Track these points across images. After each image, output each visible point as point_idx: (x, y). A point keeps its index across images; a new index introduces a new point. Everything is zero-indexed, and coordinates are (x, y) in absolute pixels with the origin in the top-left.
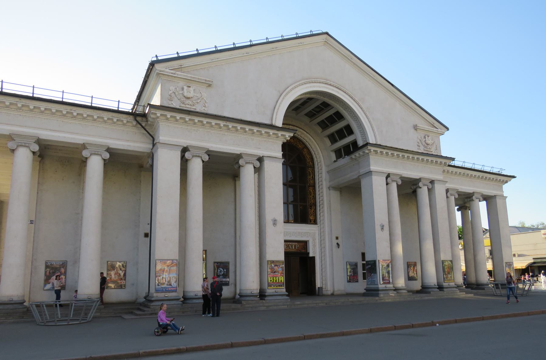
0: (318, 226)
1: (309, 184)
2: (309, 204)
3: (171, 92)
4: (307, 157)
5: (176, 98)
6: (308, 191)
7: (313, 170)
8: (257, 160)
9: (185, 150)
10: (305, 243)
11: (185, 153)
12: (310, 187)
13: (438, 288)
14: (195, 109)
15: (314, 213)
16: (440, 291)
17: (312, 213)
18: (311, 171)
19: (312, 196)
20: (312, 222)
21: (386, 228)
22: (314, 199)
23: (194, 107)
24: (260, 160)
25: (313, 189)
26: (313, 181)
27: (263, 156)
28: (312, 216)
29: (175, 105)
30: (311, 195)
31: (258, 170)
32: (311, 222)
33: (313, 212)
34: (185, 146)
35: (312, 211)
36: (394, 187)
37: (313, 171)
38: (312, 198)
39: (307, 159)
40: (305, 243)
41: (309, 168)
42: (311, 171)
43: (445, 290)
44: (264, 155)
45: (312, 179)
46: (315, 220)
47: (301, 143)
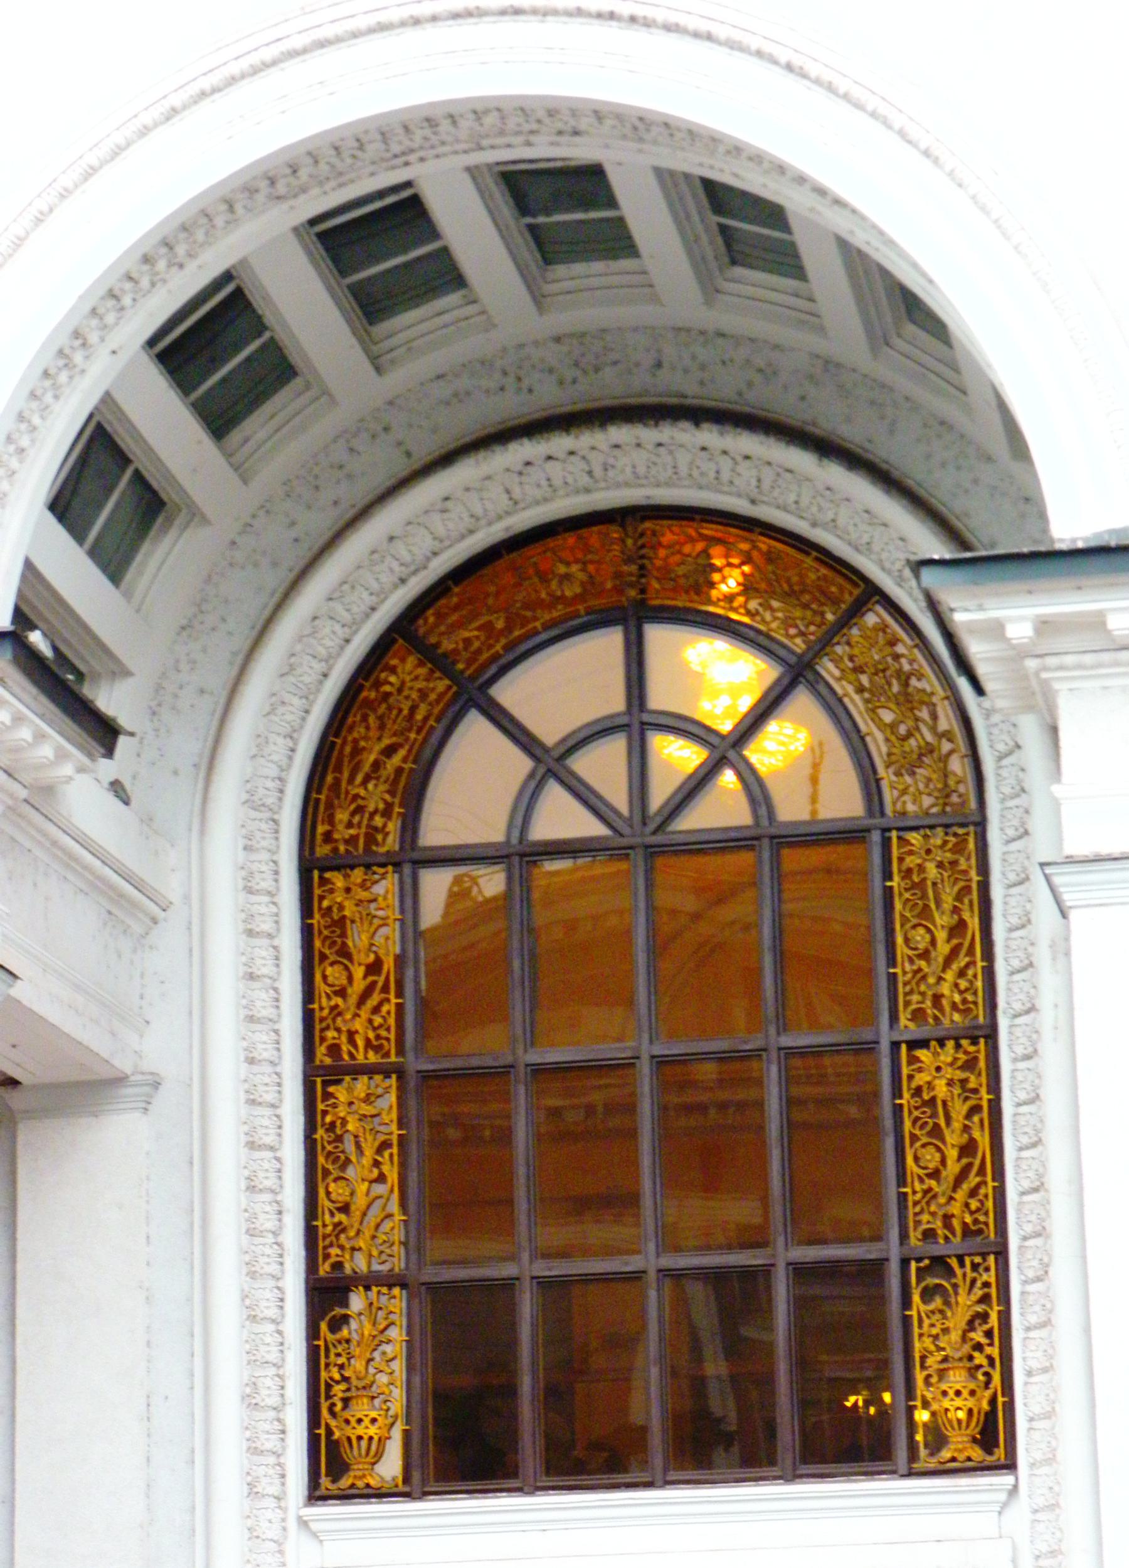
1: (918, 1015)
6: (906, 1099)
7: (960, 848)
12: (922, 1054)
15: (978, 1336)
18: (932, 871)
19: (952, 1154)
20: (960, 1445)
22: (973, 1180)
26: (962, 974)
28: (957, 1379)
30: (936, 1132)
33: (971, 1326)
35: (958, 1320)
37: (966, 863)
38: (953, 1168)
41: (914, 838)
42: (932, 871)
45: (954, 953)
46: (991, 1416)
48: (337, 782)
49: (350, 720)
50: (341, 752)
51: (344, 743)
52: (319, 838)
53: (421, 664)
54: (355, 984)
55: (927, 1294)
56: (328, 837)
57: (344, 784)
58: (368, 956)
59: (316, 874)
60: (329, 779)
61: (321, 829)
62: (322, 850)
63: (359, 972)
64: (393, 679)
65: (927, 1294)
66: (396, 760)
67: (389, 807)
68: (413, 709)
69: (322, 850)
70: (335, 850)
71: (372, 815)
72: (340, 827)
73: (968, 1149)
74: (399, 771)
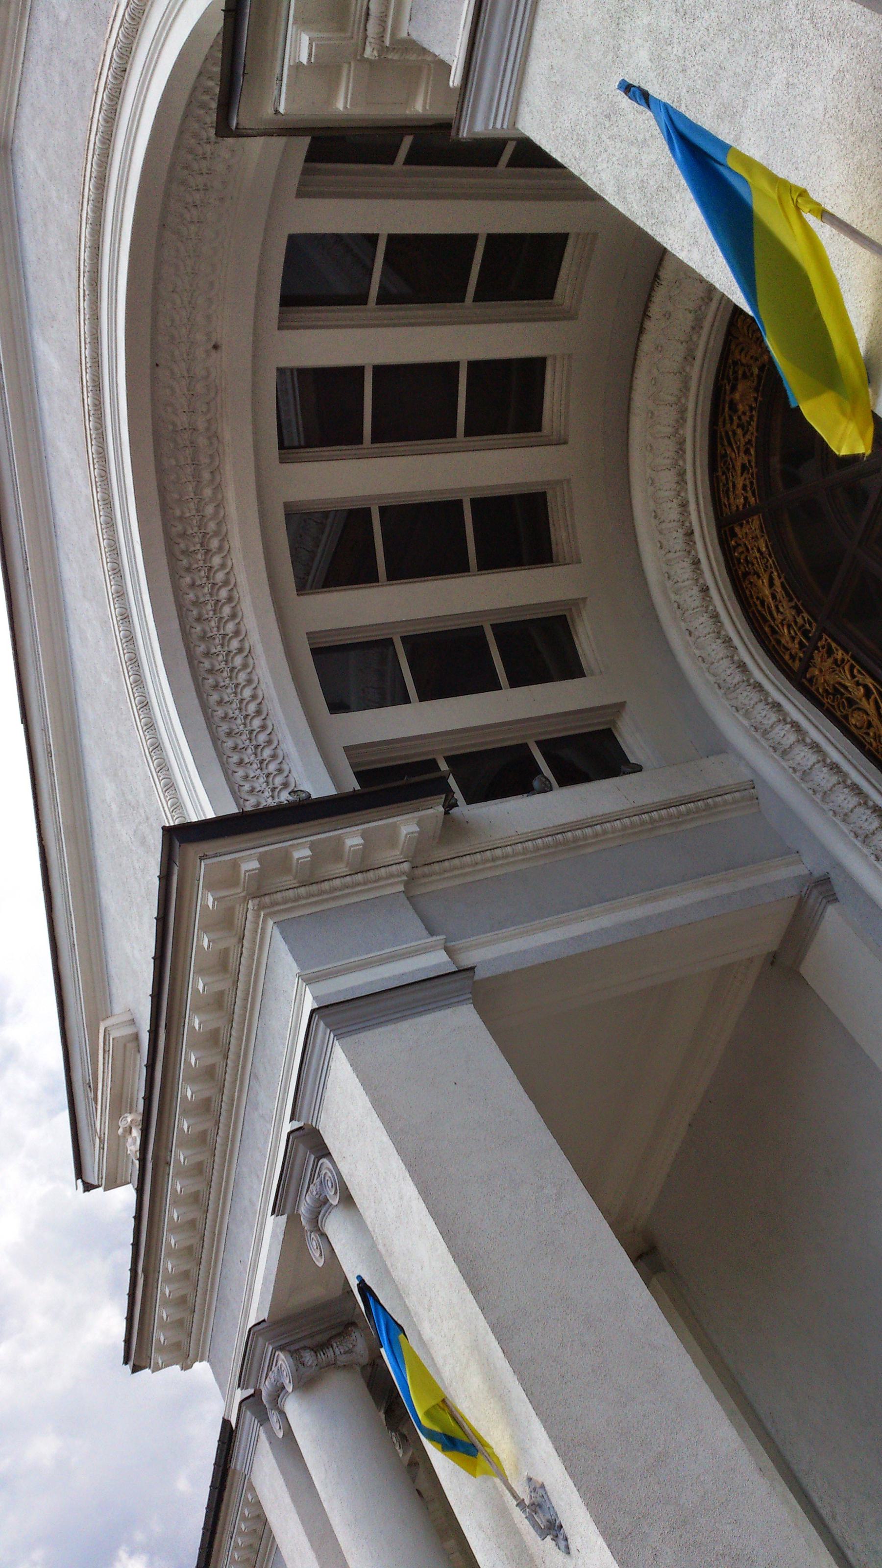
48: (771, 627)
49: (748, 593)
50: (759, 612)
51: (756, 605)
52: (790, 662)
53: (741, 525)
54: (869, 712)
56: (793, 657)
57: (772, 624)
58: (859, 690)
59: (804, 680)
60: (767, 629)
61: (787, 657)
62: (796, 665)
63: (864, 703)
64: (741, 549)
66: (777, 582)
67: (796, 607)
68: (759, 550)
69: (796, 665)
70: (800, 659)
71: (796, 622)
72: (790, 645)
74: (782, 583)
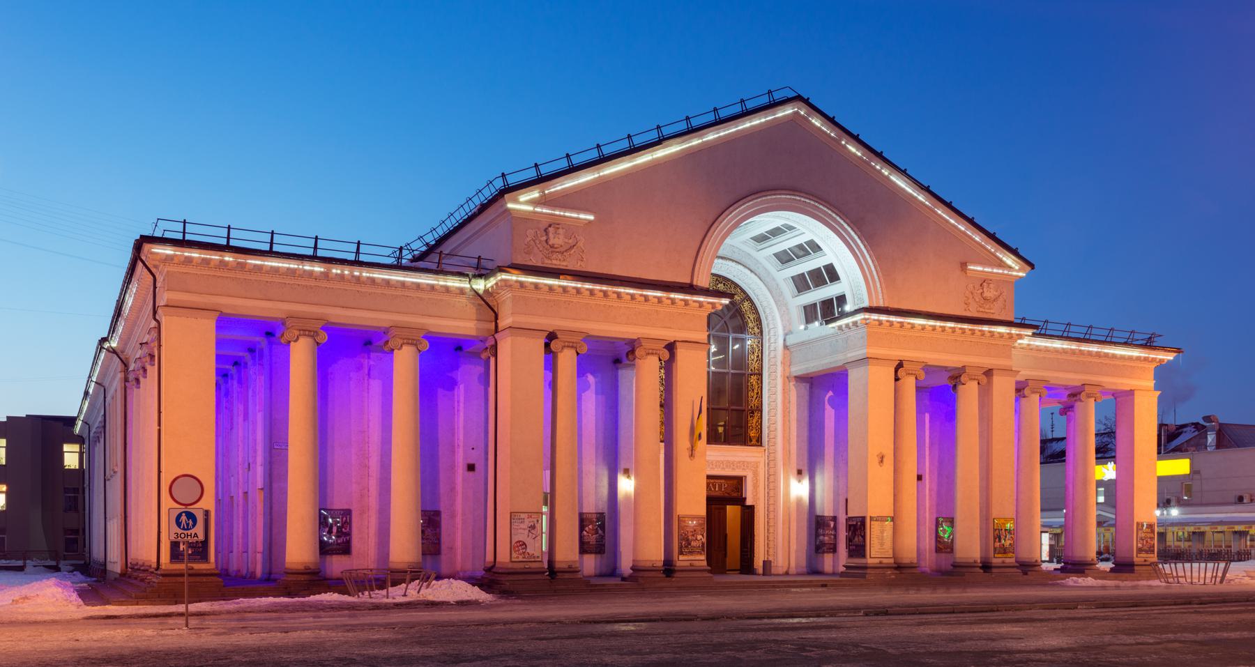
0: (765, 450)
1: (751, 370)
2: (749, 407)
3: (528, 239)
4: (749, 318)
5: (536, 248)
8: (665, 347)
9: (552, 336)
10: (739, 481)
11: (551, 341)
12: (752, 377)
13: (981, 568)
14: (566, 266)
16: (984, 572)
17: (754, 425)
20: (754, 442)
21: (889, 460)
23: (564, 264)
24: (671, 347)
25: (758, 379)
27: (675, 341)
29: (534, 262)
30: (753, 390)
31: (668, 366)
32: (751, 441)
34: (551, 330)
35: (755, 421)
36: (909, 385)
38: (755, 396)
39: (749, 321)
40: (739, 481)
43: (994, 570)
44: (677, 339)
46: (758, 437)
47: (739, 291)
55: (751, 417)
65: (751, 417)
73: (757, 393)
